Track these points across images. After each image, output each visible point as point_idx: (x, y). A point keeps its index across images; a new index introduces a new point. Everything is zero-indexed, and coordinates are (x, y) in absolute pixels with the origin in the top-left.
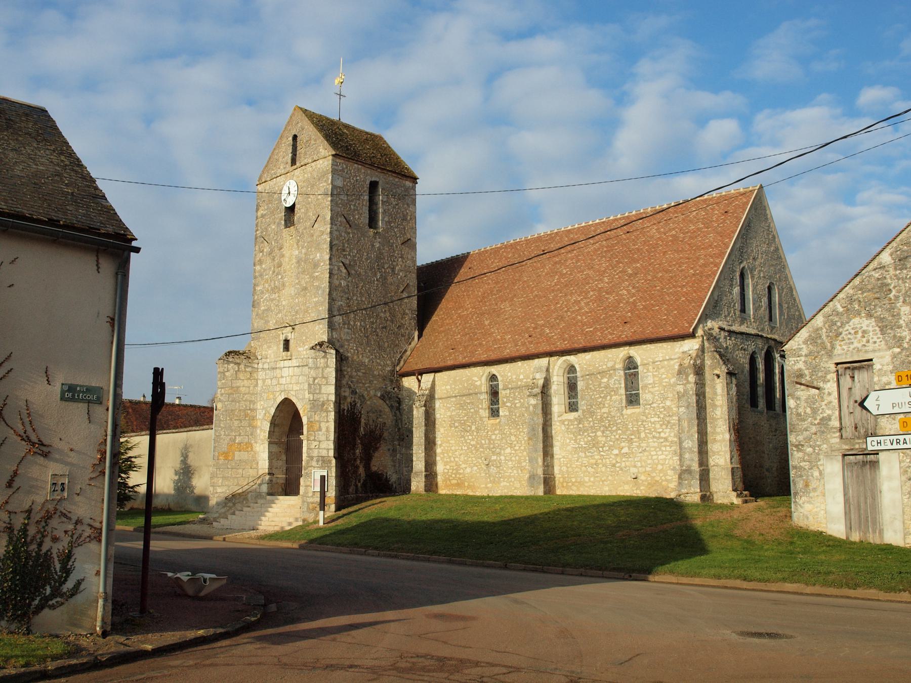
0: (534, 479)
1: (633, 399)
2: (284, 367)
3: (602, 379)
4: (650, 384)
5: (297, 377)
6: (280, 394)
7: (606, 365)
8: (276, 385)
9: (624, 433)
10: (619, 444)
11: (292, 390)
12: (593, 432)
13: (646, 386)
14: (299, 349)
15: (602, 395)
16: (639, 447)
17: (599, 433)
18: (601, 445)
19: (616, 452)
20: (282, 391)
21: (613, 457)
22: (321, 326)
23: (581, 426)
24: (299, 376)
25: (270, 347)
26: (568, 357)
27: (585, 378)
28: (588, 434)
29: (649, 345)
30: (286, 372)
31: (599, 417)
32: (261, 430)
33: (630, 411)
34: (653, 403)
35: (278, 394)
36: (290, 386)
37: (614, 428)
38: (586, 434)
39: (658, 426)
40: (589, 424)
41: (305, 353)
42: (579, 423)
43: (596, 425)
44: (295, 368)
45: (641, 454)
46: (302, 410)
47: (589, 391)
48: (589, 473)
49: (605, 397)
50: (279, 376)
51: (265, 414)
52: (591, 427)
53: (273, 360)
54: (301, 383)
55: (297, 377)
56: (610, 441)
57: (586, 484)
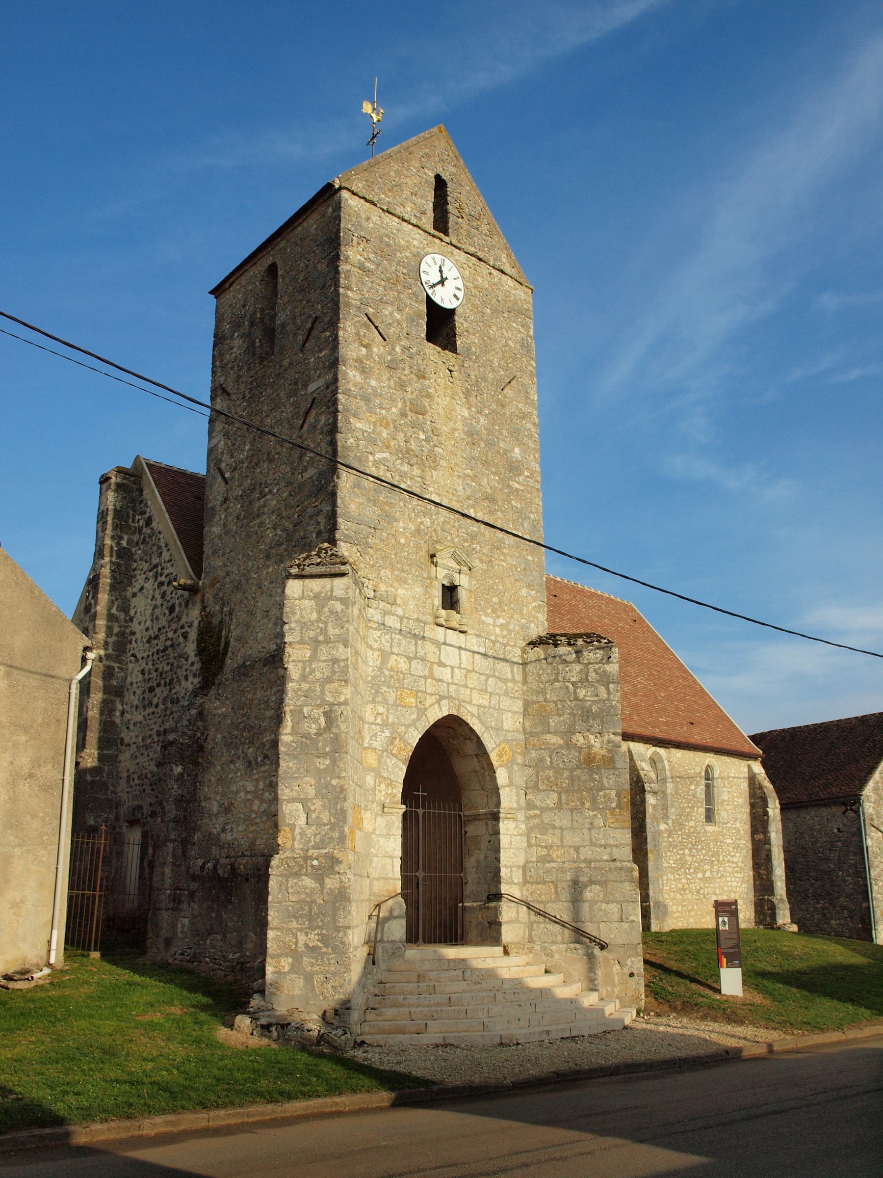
0: (659, 907)
1: (710, 816)
2: (445, 644)
3: (690, 785)
4: (726, 801)
5: (483, 678)
6: (438, 702)
7: (694, 769)
8: (425, 678)
9: (706, 854)
10: (703, 866)
11: (470, 703)
12: (681, 849)
13: (722, 803)
14: (483, 618)
15: (690, 805)
16: (718, 871)
17: (687, 851)
18: (687, 866)
19: (700, 875)
20: (442, 698)
21: (697, 881)
22: (533, 593)
23: (670, 839)
24: (488, 676)
25: (405, 582)
26: (658, 749)
27: (674, 779)
28: (677, 851)
29: (726, 758)
30: (450, 656)
31: (687, 831)
32: (379, 776)
33: (710, 828)
34: (728, 822)
35: (430, 700)
36: (462, 690)
37: (700, 847)
38: (675, 850)
39: (731, 849)
40: (678, 838)
41: (498, 631)
42: (669, 836)
43: (684, 841)
44: (477, 657)
45: (720, 880)
46: (496, 751)
47: (679, 797)
48: (677, 900)
49: (692, 808)
50: (432, 658)
51: (392, 740)
52: (680, 842)
53: (415, 616)
54: (491, 694)
55: (483, 678)
56: (696, 862)
57: (674, 915)
